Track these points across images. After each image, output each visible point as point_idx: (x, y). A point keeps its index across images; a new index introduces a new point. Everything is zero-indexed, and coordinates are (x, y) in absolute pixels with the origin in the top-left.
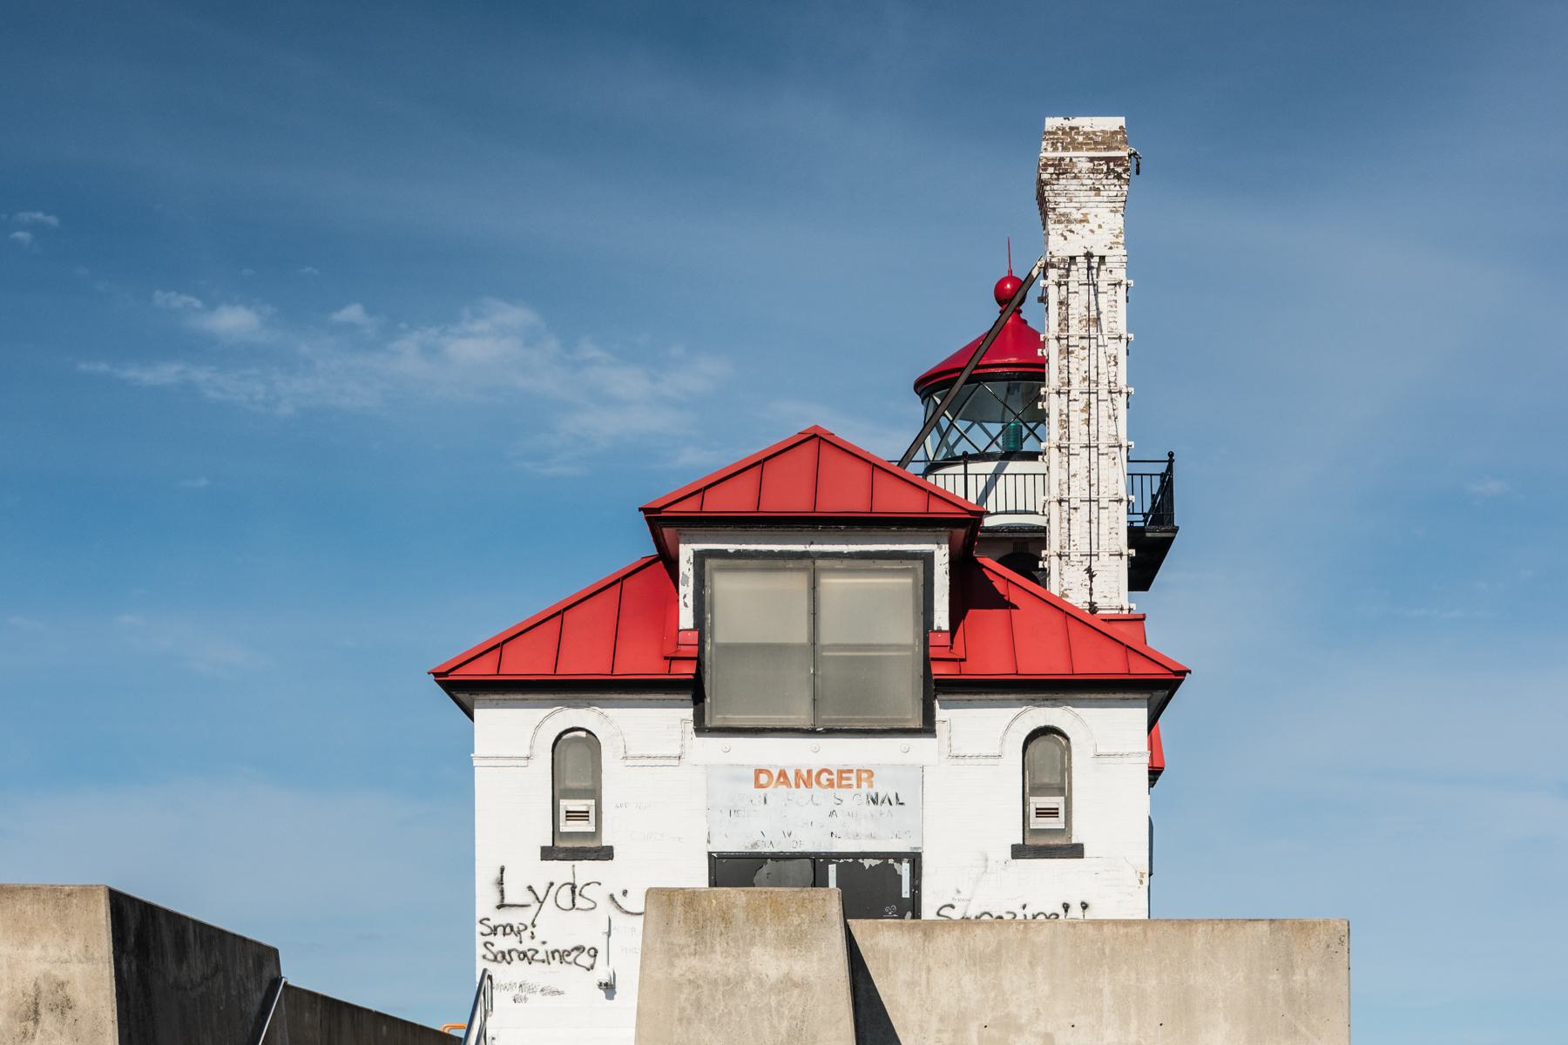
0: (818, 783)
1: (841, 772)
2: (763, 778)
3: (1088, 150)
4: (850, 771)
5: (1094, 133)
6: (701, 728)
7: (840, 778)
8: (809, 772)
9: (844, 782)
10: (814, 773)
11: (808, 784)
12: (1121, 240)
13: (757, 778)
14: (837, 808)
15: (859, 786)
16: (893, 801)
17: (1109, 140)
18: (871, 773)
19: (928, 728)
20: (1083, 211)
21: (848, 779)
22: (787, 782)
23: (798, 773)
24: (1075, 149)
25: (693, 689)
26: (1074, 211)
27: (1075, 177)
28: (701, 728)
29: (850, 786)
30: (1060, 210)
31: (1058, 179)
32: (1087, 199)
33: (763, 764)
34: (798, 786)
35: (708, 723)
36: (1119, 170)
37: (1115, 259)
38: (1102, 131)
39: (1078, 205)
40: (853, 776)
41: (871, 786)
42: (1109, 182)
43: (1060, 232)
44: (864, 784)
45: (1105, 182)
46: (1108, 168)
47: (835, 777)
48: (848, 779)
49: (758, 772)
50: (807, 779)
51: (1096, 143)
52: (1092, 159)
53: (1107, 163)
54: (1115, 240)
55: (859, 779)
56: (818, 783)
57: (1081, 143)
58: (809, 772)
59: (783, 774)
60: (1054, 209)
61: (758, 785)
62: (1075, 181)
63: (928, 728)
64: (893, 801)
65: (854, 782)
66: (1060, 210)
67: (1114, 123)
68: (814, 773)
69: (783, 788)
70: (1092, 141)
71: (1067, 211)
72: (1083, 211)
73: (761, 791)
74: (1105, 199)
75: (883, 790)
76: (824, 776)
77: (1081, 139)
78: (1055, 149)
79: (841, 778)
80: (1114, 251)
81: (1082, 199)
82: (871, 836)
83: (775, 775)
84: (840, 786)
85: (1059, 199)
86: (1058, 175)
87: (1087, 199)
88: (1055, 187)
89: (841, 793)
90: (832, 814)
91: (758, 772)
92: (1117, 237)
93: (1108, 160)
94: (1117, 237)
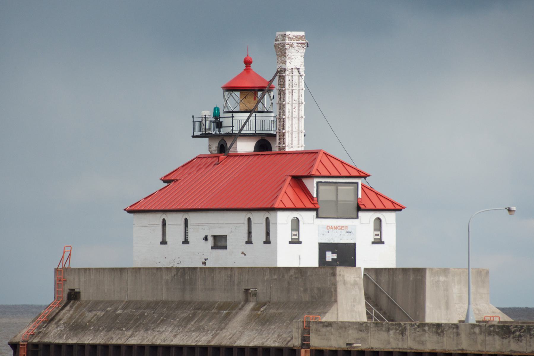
0: (338, 229)
1: (342, 226)
2: (328, 228)
3: (296, 41)
4: (343, 226)
5: (297, 36)
6: (317, 216)
7: (342, 228)
8: (336, 226)
9: (343, 229)
10: (337, 227)
11: (336, 229)
12: (303, 64)
13: (327, 228)
14: (341, 234)
15: (345, 229)
16: (351, 232)
17: (301, 38)
18: (347, 227)
19: (357, 217)
20: (294, 56)
21: (343, 228)
22: (332, 229)
23: (334, 227)
24: (293, 40)
25: (316, 210)
26: (292, 56)
27: (293, 48)
28: (317, 216)
29: (343, 229)
30: (289, 56)
31: (289, 48)
32: (295, 53)
33: (328, 225)
34: (334, 229)
35: (319, 216)
36: (304, 46)
37: (302, 69)
38: (300, 36)
39: (293, 55)
40: (344, 227)
41: (347, 229)
42: (301, 49)
43: (289, 62)
44: (346, 229)
45: (300, 49)
46: (301, 46)
47: (341, 227)
48: (343, 228)
49: (327, 226)
50: (336, 228)
51: (298, 39)
52: (297, 43)
53: (301, 44)
54: (302, 64)
55: (345, 228)
56: (338, 229)
57: (294, 39)
58: (336, 226)
59: (332, 227)
60: (288, 56)
61: (327, 229)
62: (293, 49)
63: (357, 217)
64: (351, 232)
65: (344, 228)
66: (289, 56)
67: (302, 33)
68: (337, 227)
69: (332, 230)
70: (297, 38)
71: (291, 56)
72: (294, 56)
73: (328, 230)
74: (300, 53)
75: (349, 230)
76: (339, 227)
77: (294, 37)
78: (289, 40)
79: (342, 228)
80: (301, 67)
81: (295, 53)
82: (347, 240)
83: (330, 226)
84: (342, 229)
85: (289, 53)
86: (289, 47)
87: (295, 53)
88: (289, 50)
89: (342, 231)
90: (340, 235)
91: (327, 226)
92: (302, 63)
93: (301, 43)
94: (302, 63)
